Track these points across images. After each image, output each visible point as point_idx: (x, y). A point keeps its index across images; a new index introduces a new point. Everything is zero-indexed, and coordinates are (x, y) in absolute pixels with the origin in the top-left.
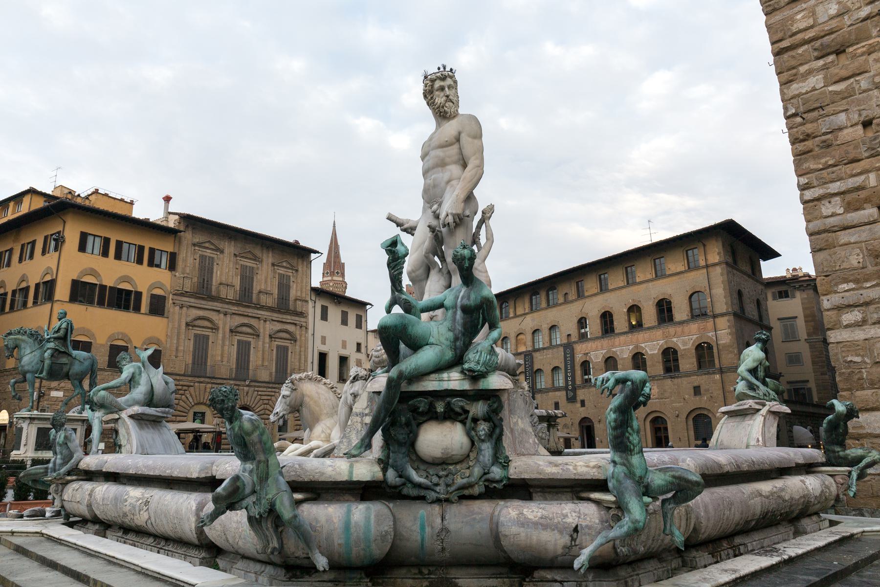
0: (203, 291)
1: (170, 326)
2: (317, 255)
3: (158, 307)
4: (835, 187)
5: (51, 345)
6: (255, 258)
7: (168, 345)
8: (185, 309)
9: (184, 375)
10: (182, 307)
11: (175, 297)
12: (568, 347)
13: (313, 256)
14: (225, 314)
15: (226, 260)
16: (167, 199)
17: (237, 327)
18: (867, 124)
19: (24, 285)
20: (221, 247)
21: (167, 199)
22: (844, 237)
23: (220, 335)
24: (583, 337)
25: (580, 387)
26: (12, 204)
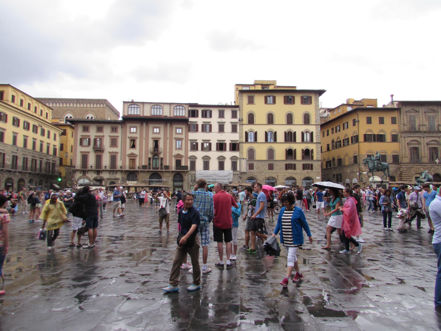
0: (413, 131)
1: (401, 145)
3: (395, 139)
5: (376, 162)
6: (434, 111)
7: (401, 153)
8: (406, 138)
9: (409, 163)
10: (404, 137)
11: (402, 134)
14: (423, 137)
15: (421, 115)
16: (392, 96)
17: (429, 142)
19: (346, 137)
20: (418, 110)
21: (392, 96)
23: (422, 146)
26: (336, 110)
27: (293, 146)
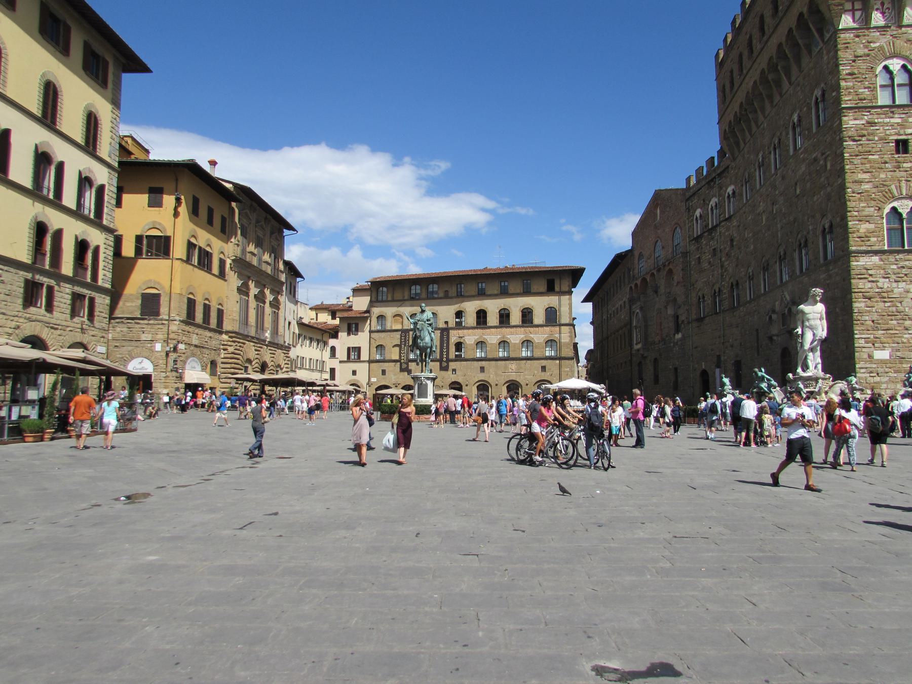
2: (292, 232)
4: (863, 336)
12: (445, 332)
13: (286, 232)
18: (873, 321)
22: (864, 350)
24: (459, 326)
25: (452, 361)
27: (55, 219)
